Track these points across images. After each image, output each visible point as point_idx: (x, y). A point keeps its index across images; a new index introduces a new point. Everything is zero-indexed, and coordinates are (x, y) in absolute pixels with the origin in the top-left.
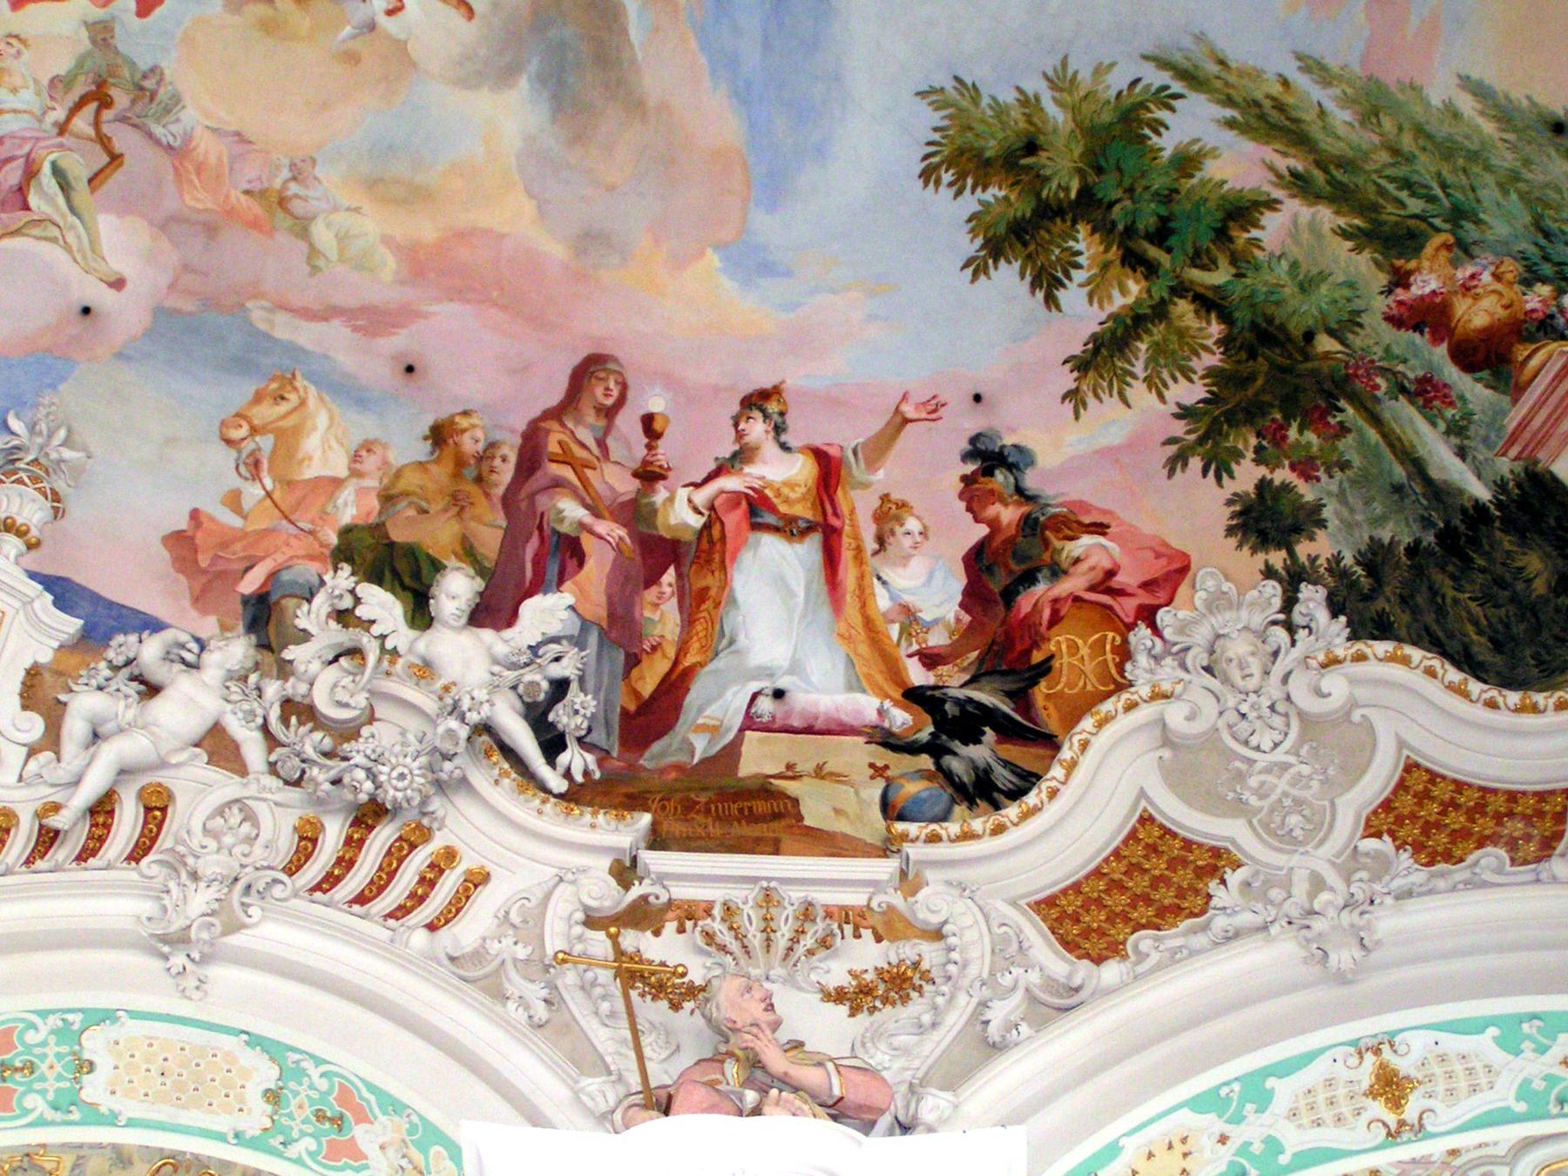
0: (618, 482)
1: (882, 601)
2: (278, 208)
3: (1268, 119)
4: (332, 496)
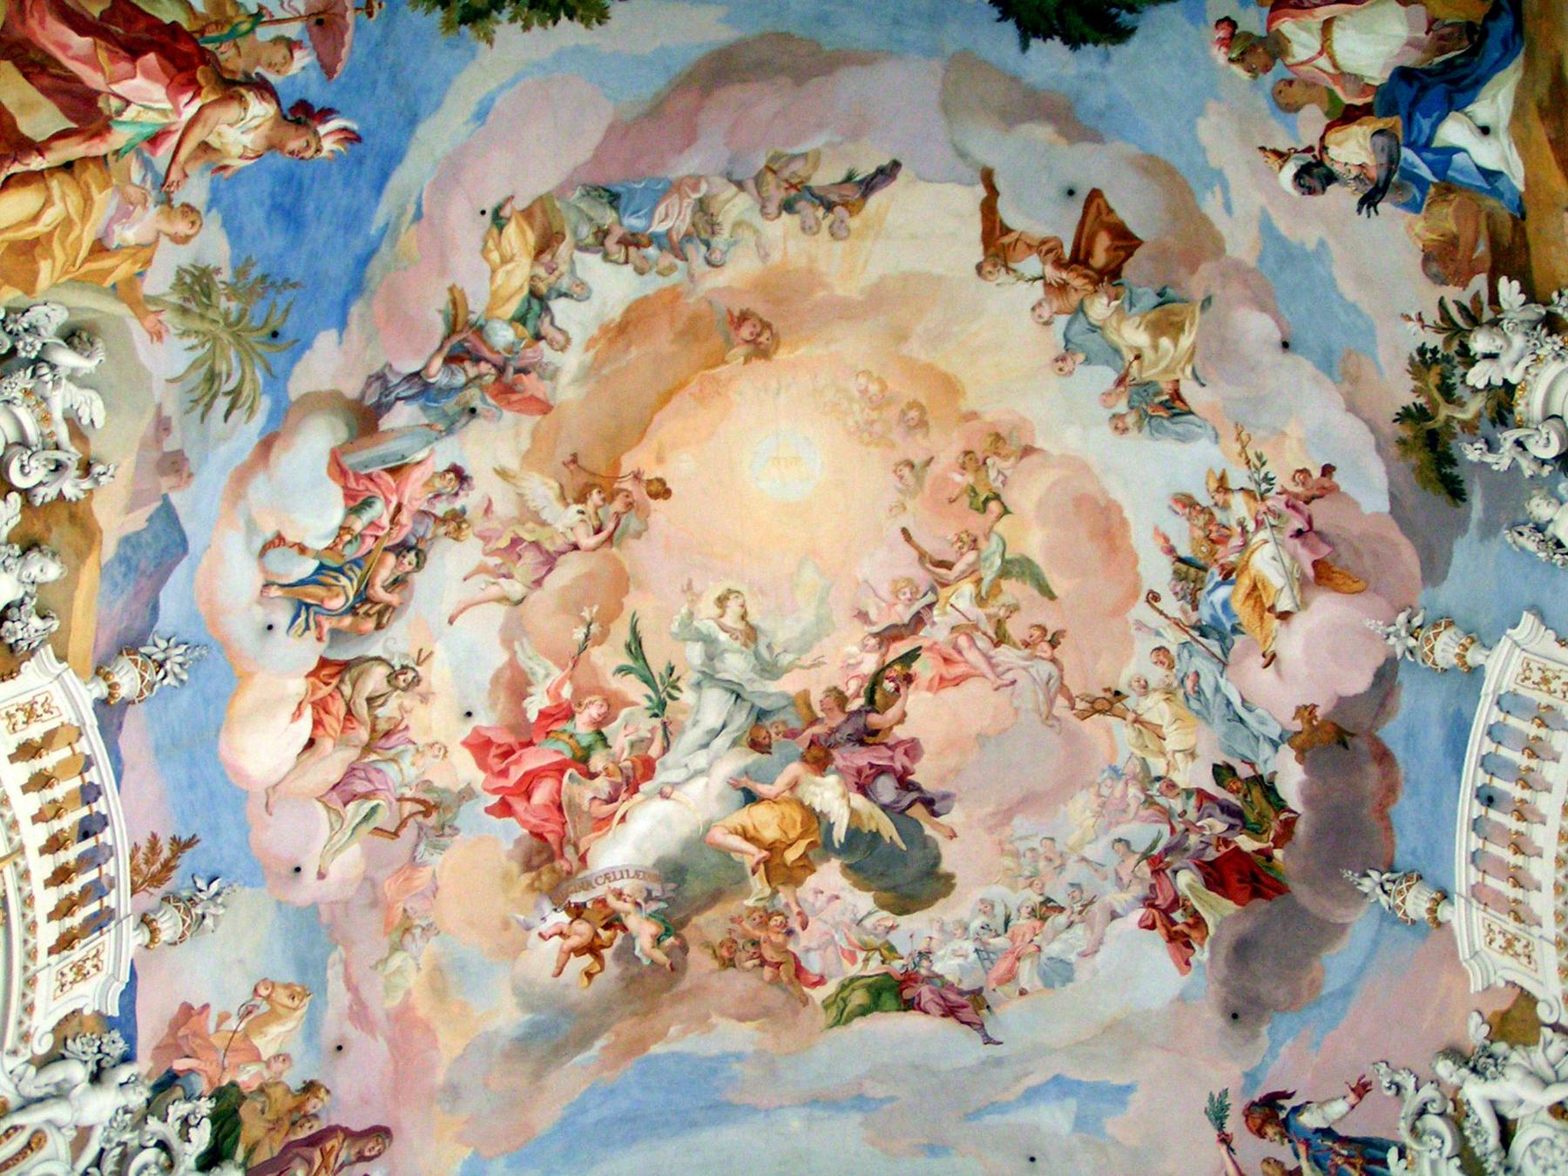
2: (403, 930)
4: (250, 1062)
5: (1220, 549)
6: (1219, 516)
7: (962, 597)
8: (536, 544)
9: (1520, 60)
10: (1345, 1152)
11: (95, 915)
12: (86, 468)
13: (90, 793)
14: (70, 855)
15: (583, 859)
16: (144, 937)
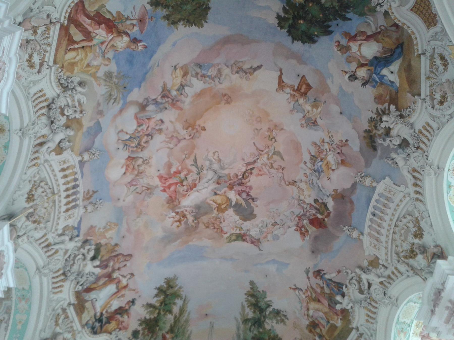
0: (117, 266)
1: (111, 302)
3: (182, 311)
5: (321, 154)
6: (321, 147)
7: (264, 158)
8: (177, 137)
9: (401, 58)
11: (74, 205)
12: (81, 112)
13: (76, 180)
14: (70, 192)
15: (179, 203)
16: (84, 210)
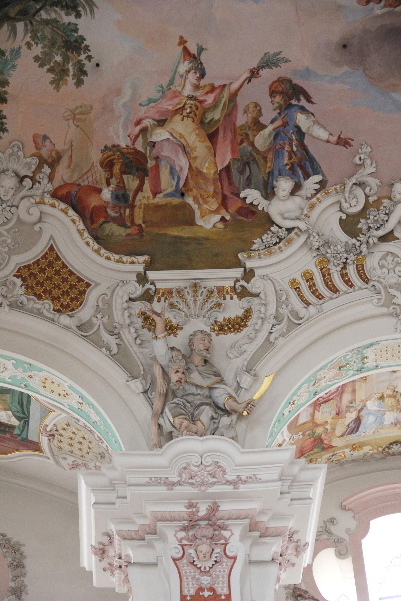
10: (295, 149)
